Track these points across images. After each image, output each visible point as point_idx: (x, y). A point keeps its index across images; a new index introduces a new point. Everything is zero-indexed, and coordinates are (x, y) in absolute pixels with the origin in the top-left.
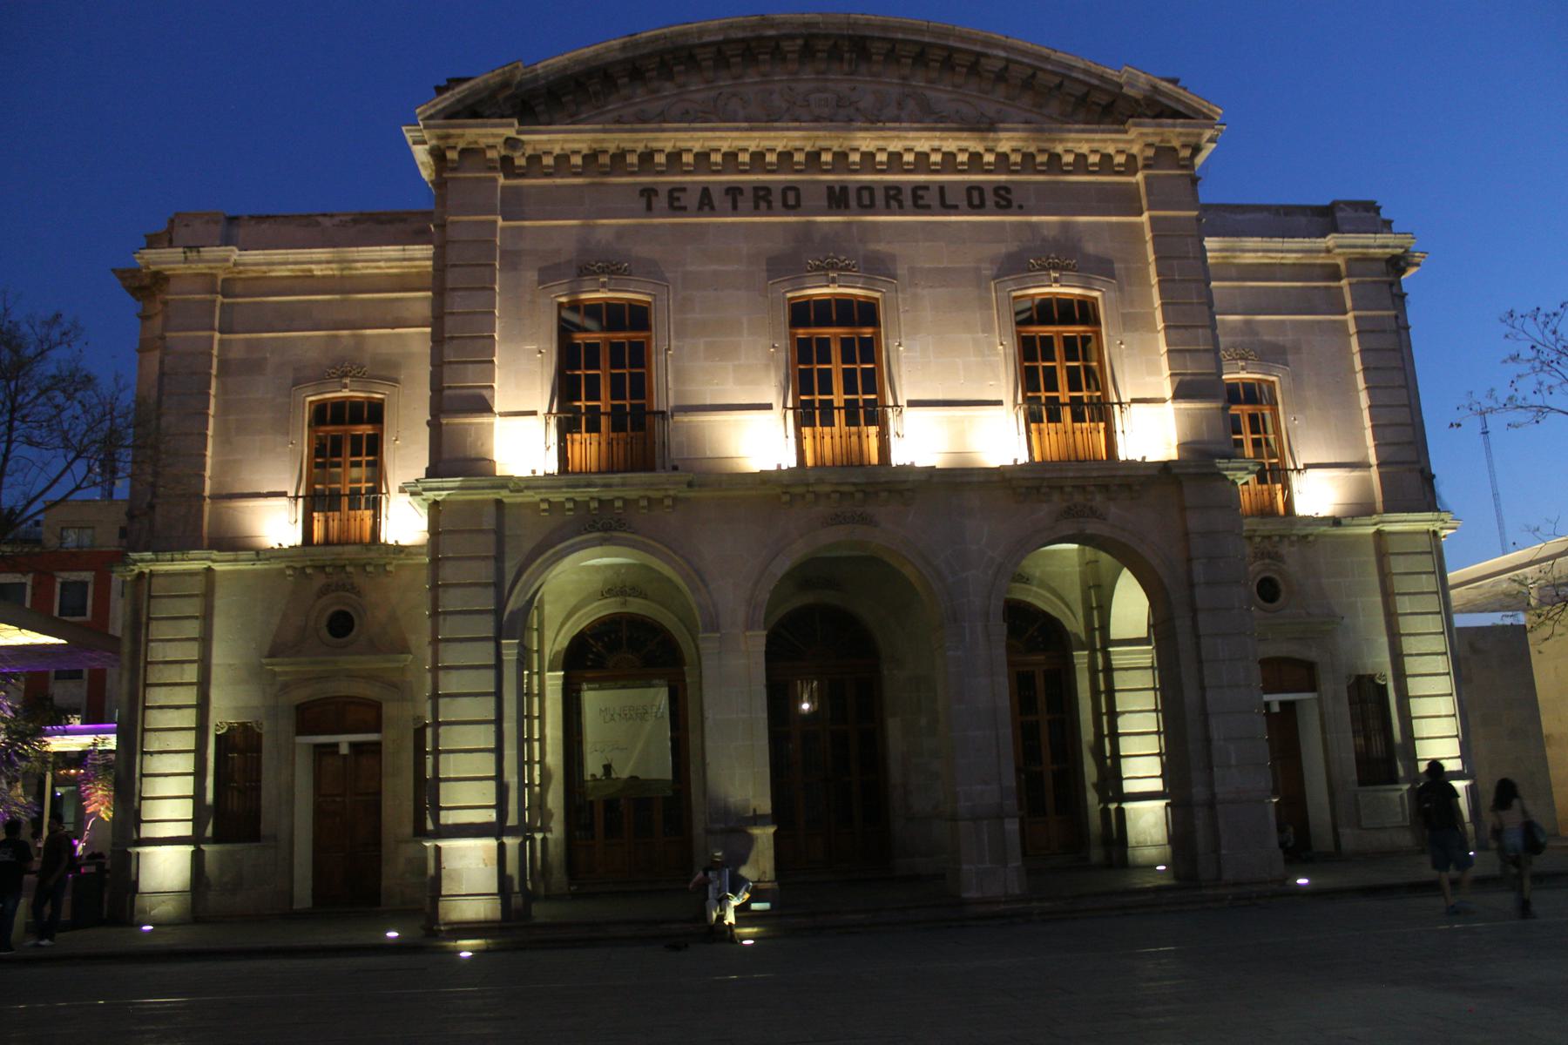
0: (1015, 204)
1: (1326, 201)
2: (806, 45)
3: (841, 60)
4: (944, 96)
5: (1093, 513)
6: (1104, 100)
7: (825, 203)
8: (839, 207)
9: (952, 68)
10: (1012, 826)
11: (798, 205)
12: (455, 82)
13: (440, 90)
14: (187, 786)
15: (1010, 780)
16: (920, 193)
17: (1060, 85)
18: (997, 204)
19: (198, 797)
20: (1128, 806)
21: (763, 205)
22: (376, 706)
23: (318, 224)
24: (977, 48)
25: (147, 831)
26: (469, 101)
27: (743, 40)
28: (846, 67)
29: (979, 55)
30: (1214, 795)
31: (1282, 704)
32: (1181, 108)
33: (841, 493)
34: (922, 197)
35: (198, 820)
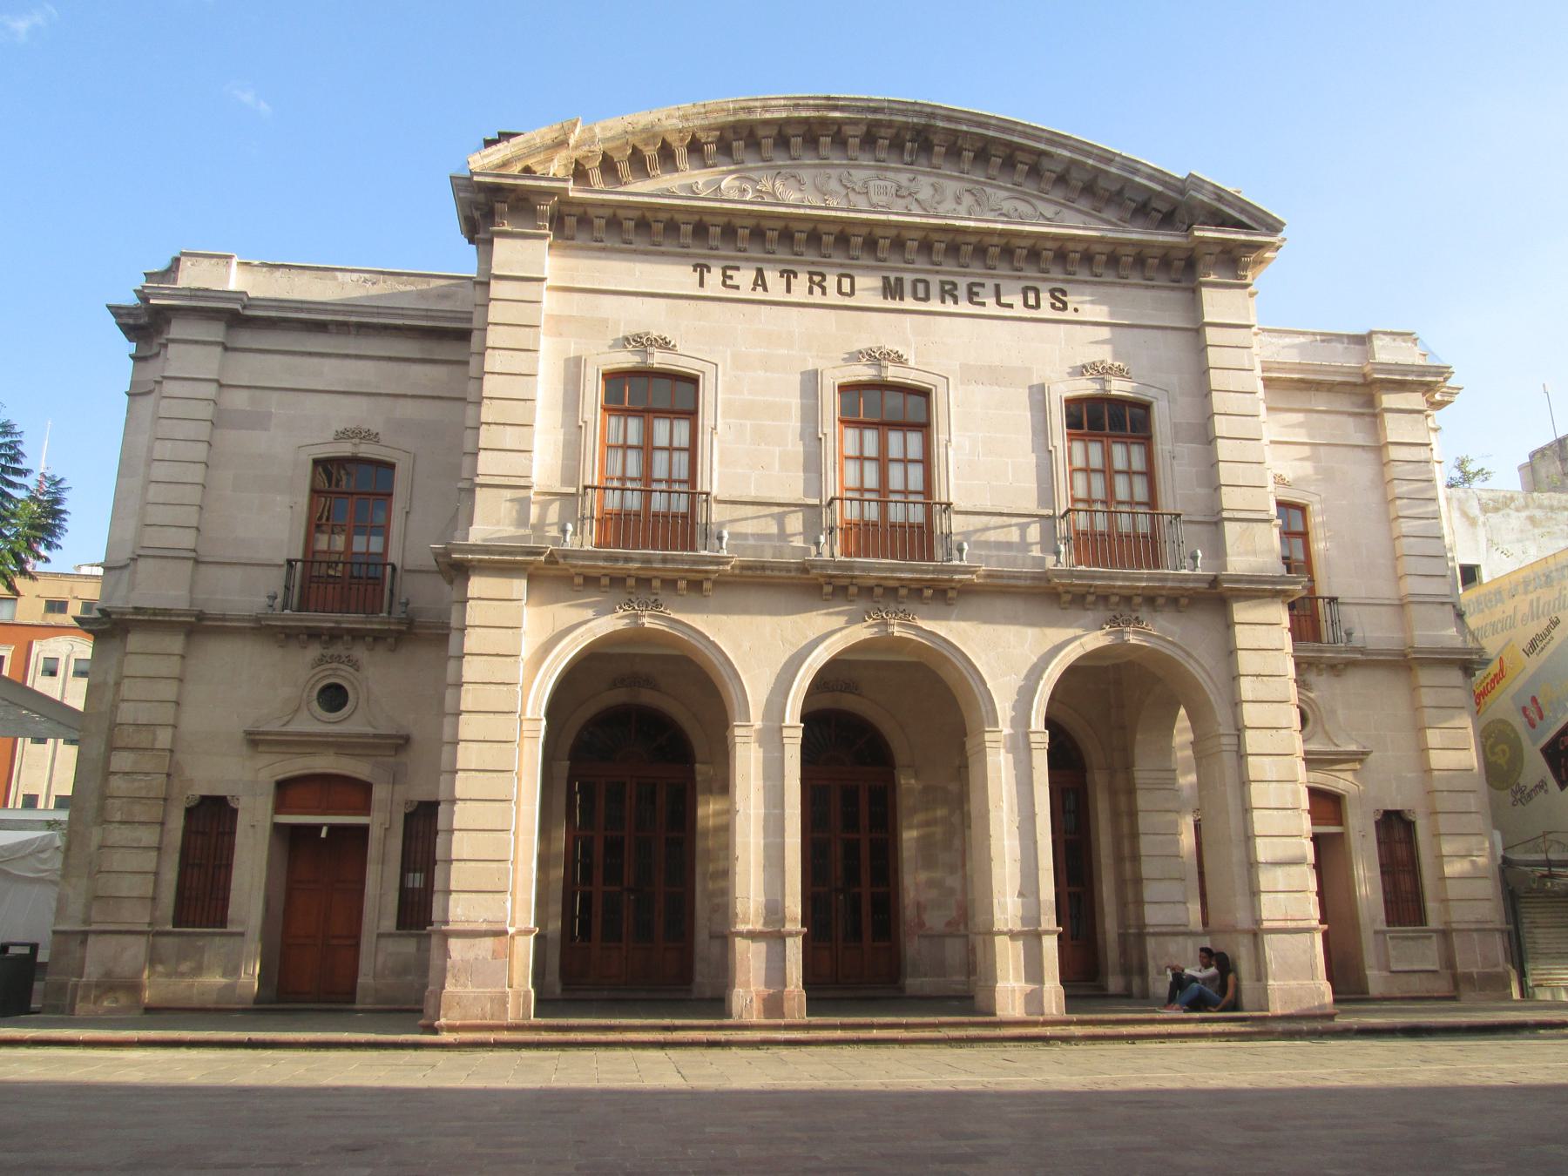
0: (1070, 307)
1: (1363, 331)
2: (868, 132)
4: (1006, 194)
6: (1164, 207)
8: (893, 298)
9: (1014, 166)
12: (505, 136)
13: (489, 143)
16: (975, 289)
17: (1120, 192)
18: (1053, 306)
21: (817, 290)
22: (366, 788)
23: (335, 279)
24: (1042, 146)
27: (806, 120)
28: (907, 158)
29: (1042, 154)
30: (1258, 921)
32: (1244, 219)
33: (886, 589)
34: (977, 294)
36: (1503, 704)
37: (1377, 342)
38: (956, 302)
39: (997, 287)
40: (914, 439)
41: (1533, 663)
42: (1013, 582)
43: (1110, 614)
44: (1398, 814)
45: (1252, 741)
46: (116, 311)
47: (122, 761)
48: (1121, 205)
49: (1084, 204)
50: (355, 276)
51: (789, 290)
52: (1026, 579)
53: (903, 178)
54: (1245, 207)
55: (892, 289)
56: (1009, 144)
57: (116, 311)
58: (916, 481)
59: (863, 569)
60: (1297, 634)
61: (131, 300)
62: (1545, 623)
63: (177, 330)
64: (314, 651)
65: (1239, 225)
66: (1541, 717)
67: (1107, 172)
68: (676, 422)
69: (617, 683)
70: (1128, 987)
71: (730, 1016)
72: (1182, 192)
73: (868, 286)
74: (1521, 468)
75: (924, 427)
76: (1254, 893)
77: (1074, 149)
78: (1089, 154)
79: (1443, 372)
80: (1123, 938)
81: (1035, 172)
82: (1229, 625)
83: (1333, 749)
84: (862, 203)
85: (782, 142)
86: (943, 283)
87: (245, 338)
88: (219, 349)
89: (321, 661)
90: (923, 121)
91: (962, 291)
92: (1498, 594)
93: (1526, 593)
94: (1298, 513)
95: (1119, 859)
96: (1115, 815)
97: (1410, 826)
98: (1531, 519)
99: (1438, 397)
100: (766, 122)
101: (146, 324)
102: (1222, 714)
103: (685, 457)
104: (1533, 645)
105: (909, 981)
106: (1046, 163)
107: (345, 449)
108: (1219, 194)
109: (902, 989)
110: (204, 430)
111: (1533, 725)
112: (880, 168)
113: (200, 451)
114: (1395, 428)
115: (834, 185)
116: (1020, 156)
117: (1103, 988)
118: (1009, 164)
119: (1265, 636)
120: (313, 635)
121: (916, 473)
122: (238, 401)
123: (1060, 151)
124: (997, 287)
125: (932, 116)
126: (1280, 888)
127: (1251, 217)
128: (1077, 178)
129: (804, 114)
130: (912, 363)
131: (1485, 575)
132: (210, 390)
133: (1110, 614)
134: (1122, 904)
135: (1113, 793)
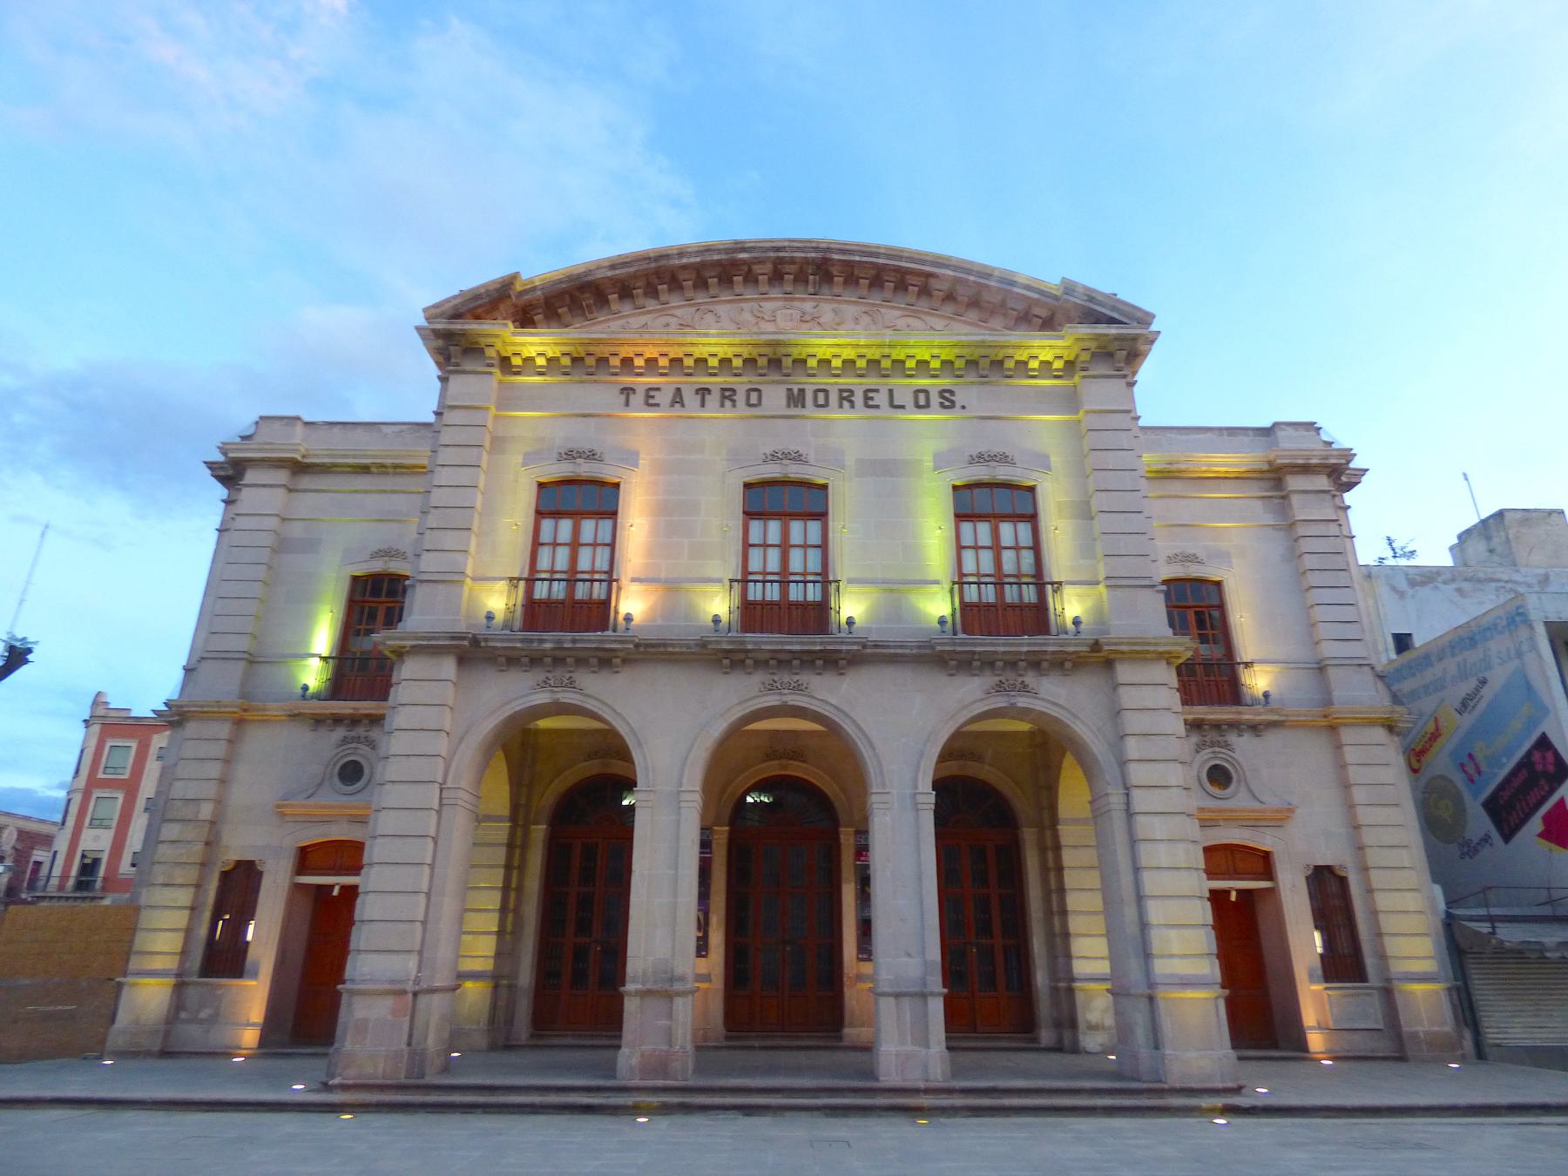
0: (958, 405)
1: (1267, 423)
3: (806, 282)
4: (898, 313)
5: (1024, 688)
6: (1044, 313)
7: (784, 402)
10: (937, 1007)
11: (760, 403)
14: (181, 919)
15: (934, 953)
17: (1003, 304)
19: (189, 932)
20: (1077, 985)
24: (927, 268)
25: (135, 963)
26: (471, 306)
27: (719, 263)
28: (811, 290)
29: (929, 275)
31: (1239, 892)
32: (1116, 315)
33: (780, 662)
35: (184, 953)
36: (1441, 762)
37: (1280, 433)
38: (853, 406)
39: (891, 391)
40: (814, 527)
41: (1468, 720)
42: (899, 651)
43: (997, 679)
44: (1329, 868)
45: (1140, 800)
46: (211, 465)
47: (170, 831)
48: (1005, 315)
49: (973, 315)
50: (397, 428)
51: (703, 405)
52: (911, 648)
53: (808, 306)
54: (1113, 301)
55: (796, 399)
56: (898, 270)
57: (211, 465)
58: (814, 564)
59: (755, 643)
60: (1189, 695)
61: (218, 457)
62: (1472, 683)
63: (250, 476)
64: (340, 733)
65: (1112, 321)
66: (1479, 773)
67: (987, 286)
68: (601, 522)
69: (593, 755)
70: (1060, 1040)
71: (614, 1077)
72: (1056, 298)
73: (775, 396)
74: (1451, 549)
75: (822, 516)
76: (1147, 956)
77: (956, 268)
78: (969, 272)
79: (1348, 455)
80: (1055, 990)
81: (925, 291)
82: (1115, 687)
83: (1257, 805)
84: (770, 327)
85: (701, 284)
86: (841, 391)
87: (305, 481)
88: (282, 491)
89: (345, 741)
90: (820, 255)
91: (858, 398)
92: (1426, 660)
93: (1453, 655)
94: (1215, 588)
95: (1049, 913)
96: (1044, 869)
97: (1343, 881)
98: (1459, 590)
99: (1344, 479)
100: (684, 267)
101: (230, 472)
102: (1110, 772)
103: (607, 550)
104: (1464, 704)
105: (846, 1031)
106: (934, 283)
107: (377, 566)
108: (1091, 295)
109: (840, 1038)
110: (265, 555)
111: (1472, 781)
112: (786, 299)
113: (261, 572)
114: (1302, 509)
115: (747, 316)
116: (910, 279)
117: (1035, 1040)
118: (901, 286)
119: (1153, 698)
120: (337, 720)
121: (814, 557)
122: (296, 530)
123: (943, 271)
124: (891, 391)
125: (829, 250)
126: (1175, 951)
127: (1122, 313)
128: (963, 294)
129: (716, 257)
130: (812, 461)
131: (1418, 642)
132: (273, 523)
133: (997, 679)
134: (1052, 957)
135: (1043, 850)
